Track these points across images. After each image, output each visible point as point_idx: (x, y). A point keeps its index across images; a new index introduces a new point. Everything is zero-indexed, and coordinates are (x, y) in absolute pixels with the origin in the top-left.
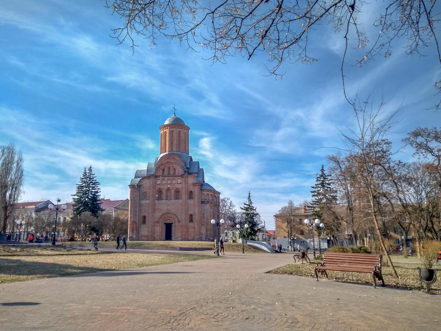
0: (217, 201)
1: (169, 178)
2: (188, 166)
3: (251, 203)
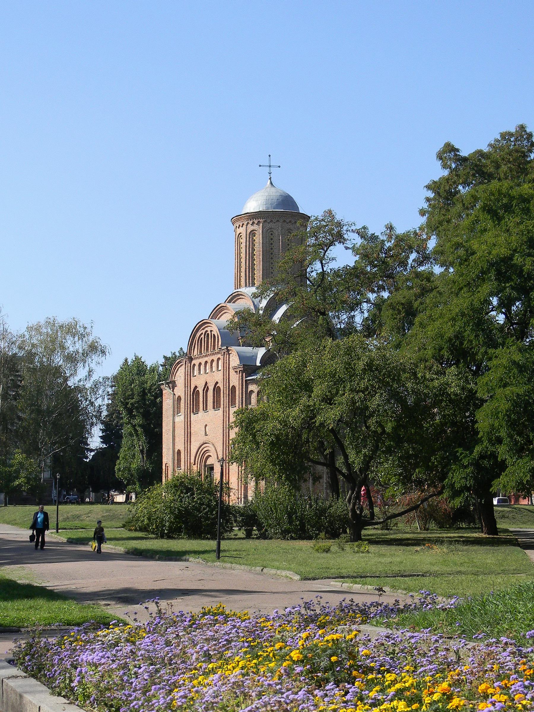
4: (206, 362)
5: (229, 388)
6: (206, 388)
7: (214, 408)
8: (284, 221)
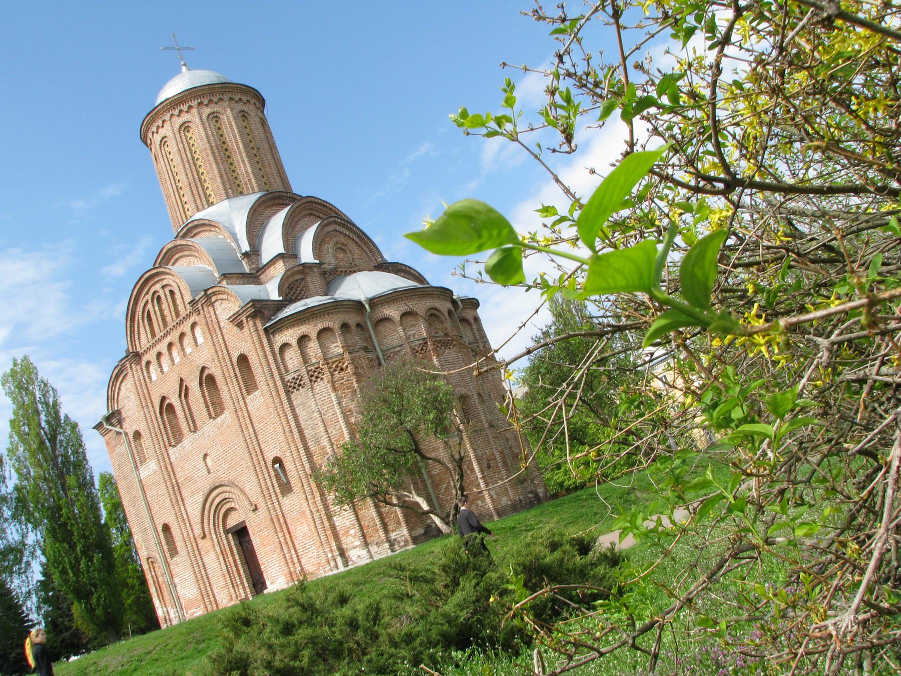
1: (169, 339)
2: (246, 247)
5: (233, 365)
6: (184, 391)
7: (211, 417)
8: (231, 99)
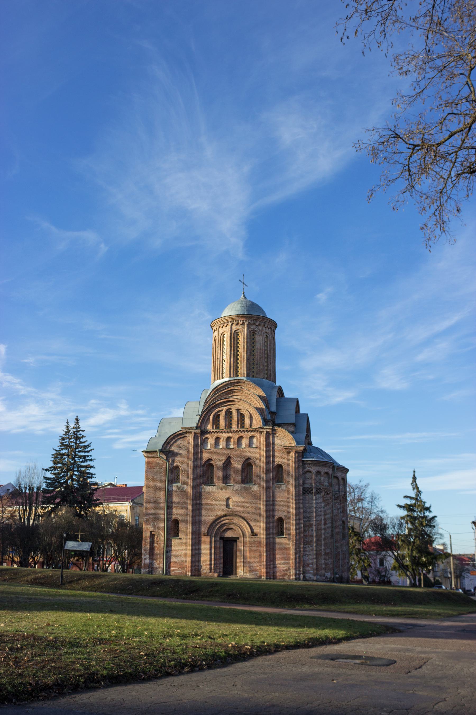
0: (341, 487)
1: (230, 435)
2: (273, 409)
3: (419, 492)
4: (229, 439)
